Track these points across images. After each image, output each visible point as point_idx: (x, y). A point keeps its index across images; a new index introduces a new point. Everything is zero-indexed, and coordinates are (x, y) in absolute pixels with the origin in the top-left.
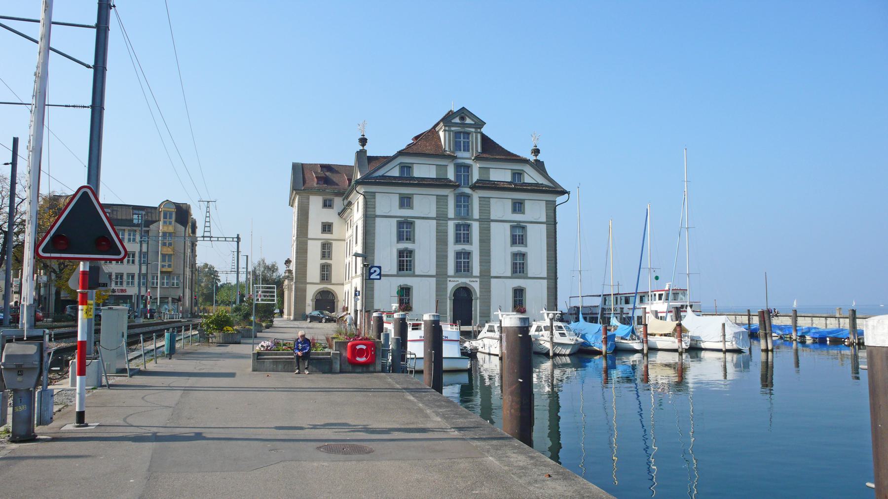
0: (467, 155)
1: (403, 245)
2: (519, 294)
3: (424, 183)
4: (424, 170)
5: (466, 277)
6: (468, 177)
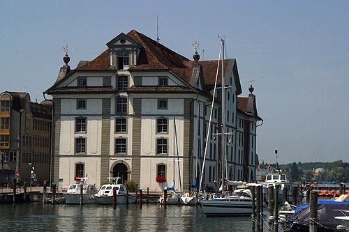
1: (81, 134)
2: (161, 169)
3: (94, 91)
4: (95, 81)
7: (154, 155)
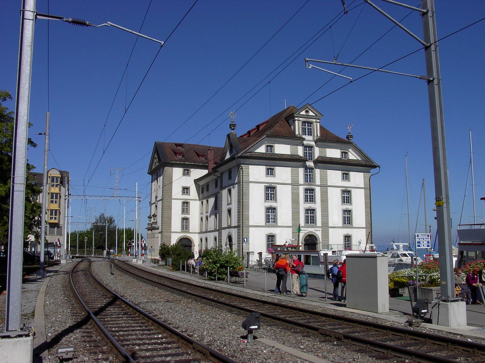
0: (310, 138)
5: (313, 227)
6: (311, 155)
7: (341, 226)
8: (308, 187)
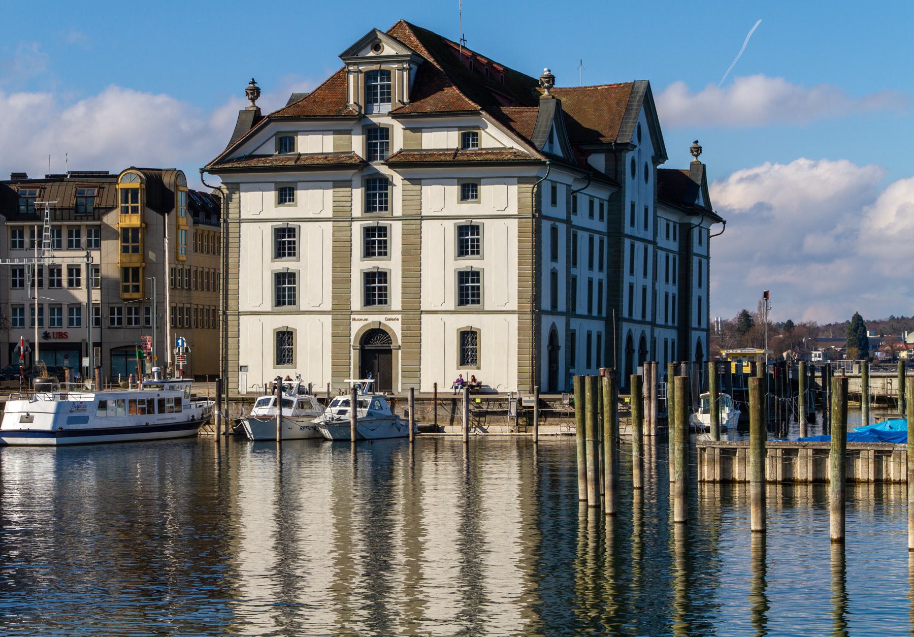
6: (386, 146)
7: (453, 308)
8: (370, 223)
